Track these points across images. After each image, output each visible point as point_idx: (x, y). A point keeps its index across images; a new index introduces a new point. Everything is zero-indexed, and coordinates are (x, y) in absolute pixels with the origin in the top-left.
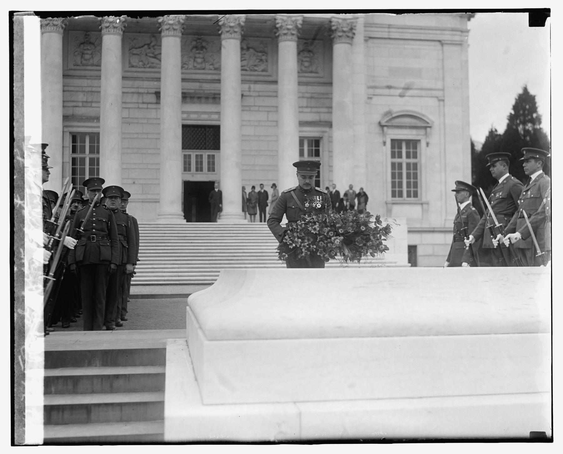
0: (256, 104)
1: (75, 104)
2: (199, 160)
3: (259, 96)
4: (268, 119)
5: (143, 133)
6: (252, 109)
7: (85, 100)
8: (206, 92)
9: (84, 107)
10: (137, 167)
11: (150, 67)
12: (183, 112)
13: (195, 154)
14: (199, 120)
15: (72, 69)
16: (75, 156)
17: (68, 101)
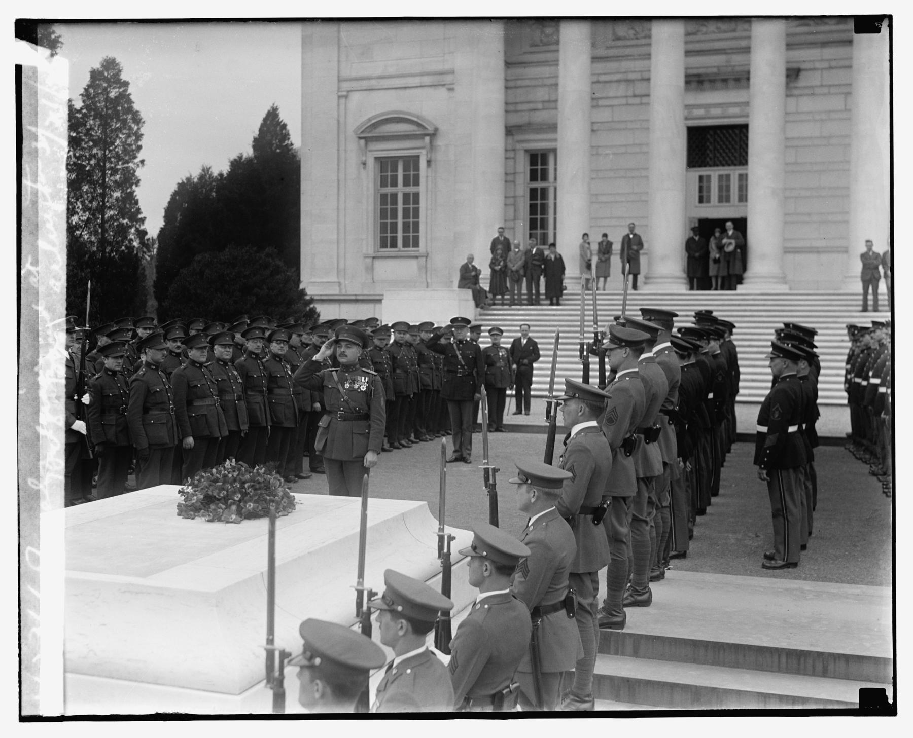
0: (824, 83)
1: (531, 106)
2: (724, 183)
3: (831, 68)
4: (845, 106)
5: (634, 145)
6: (817, 91)
7: (546, 98)
8: (737, 69)
9: (546, 109)
10: (624, 199)
11: (645, 37)
12: (687, 107)
13: (717, 173)
14: (724, 117)
15: (531, 53)
16: (535, 185)
17: (522, 103)
